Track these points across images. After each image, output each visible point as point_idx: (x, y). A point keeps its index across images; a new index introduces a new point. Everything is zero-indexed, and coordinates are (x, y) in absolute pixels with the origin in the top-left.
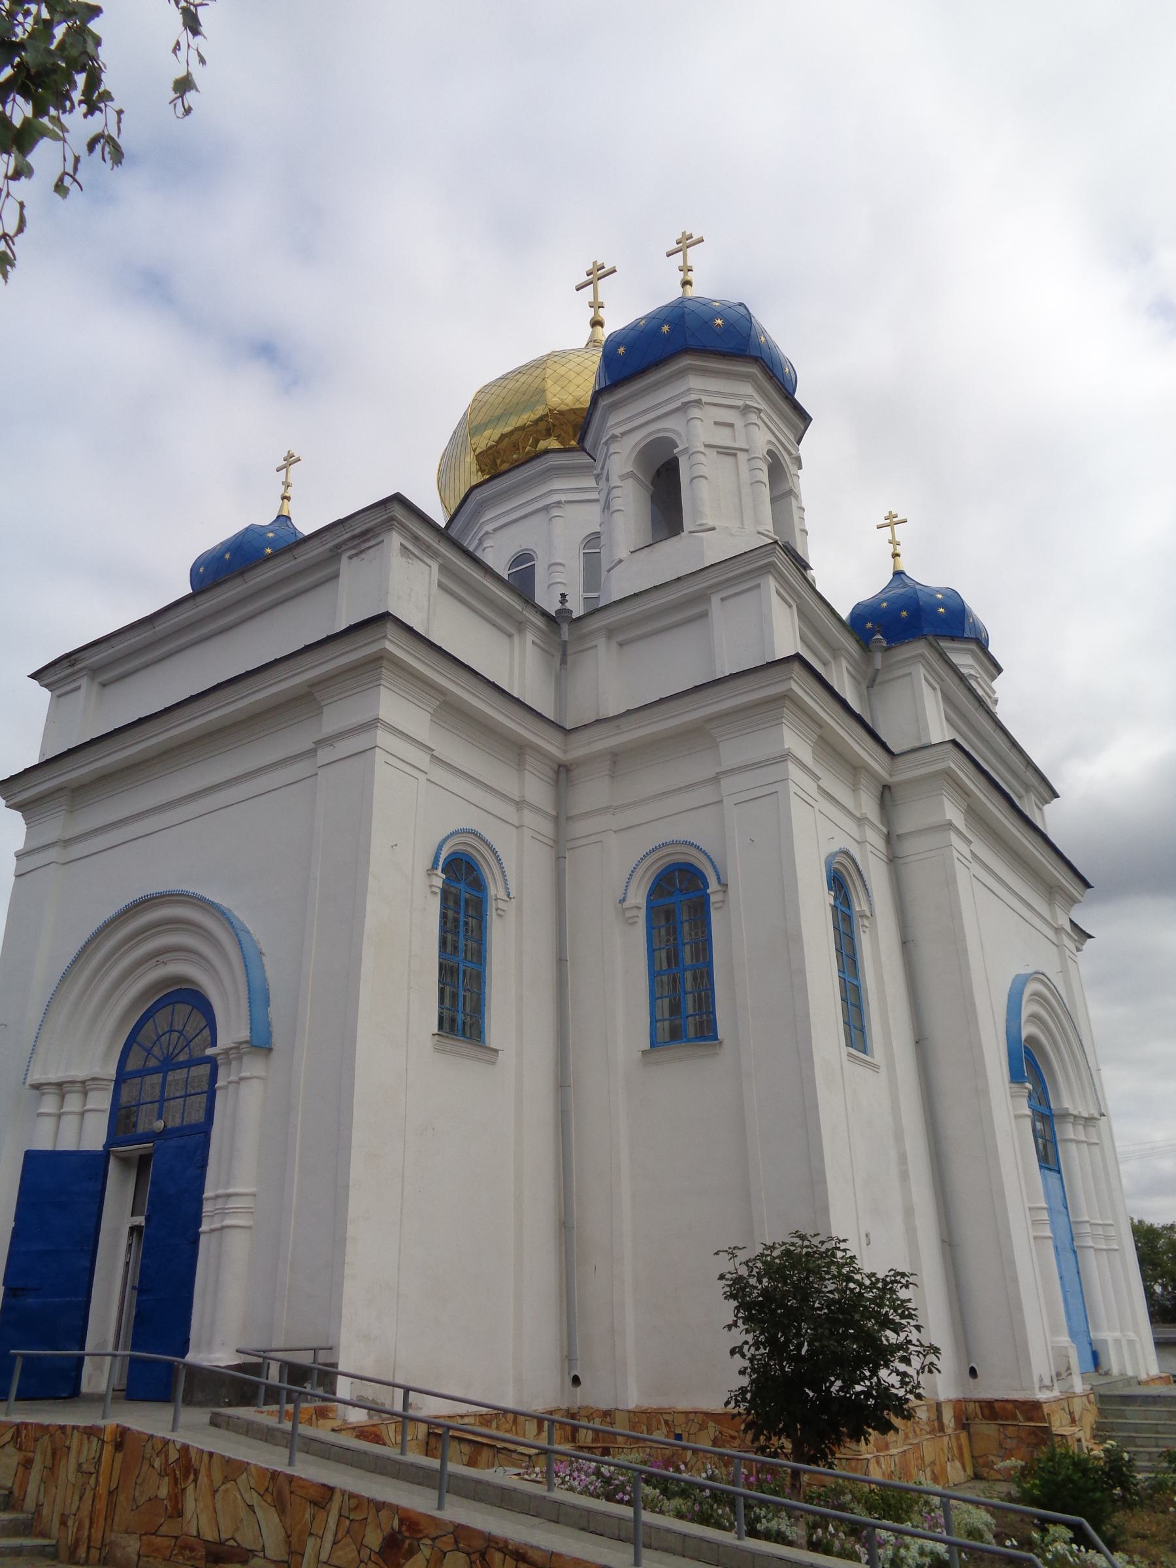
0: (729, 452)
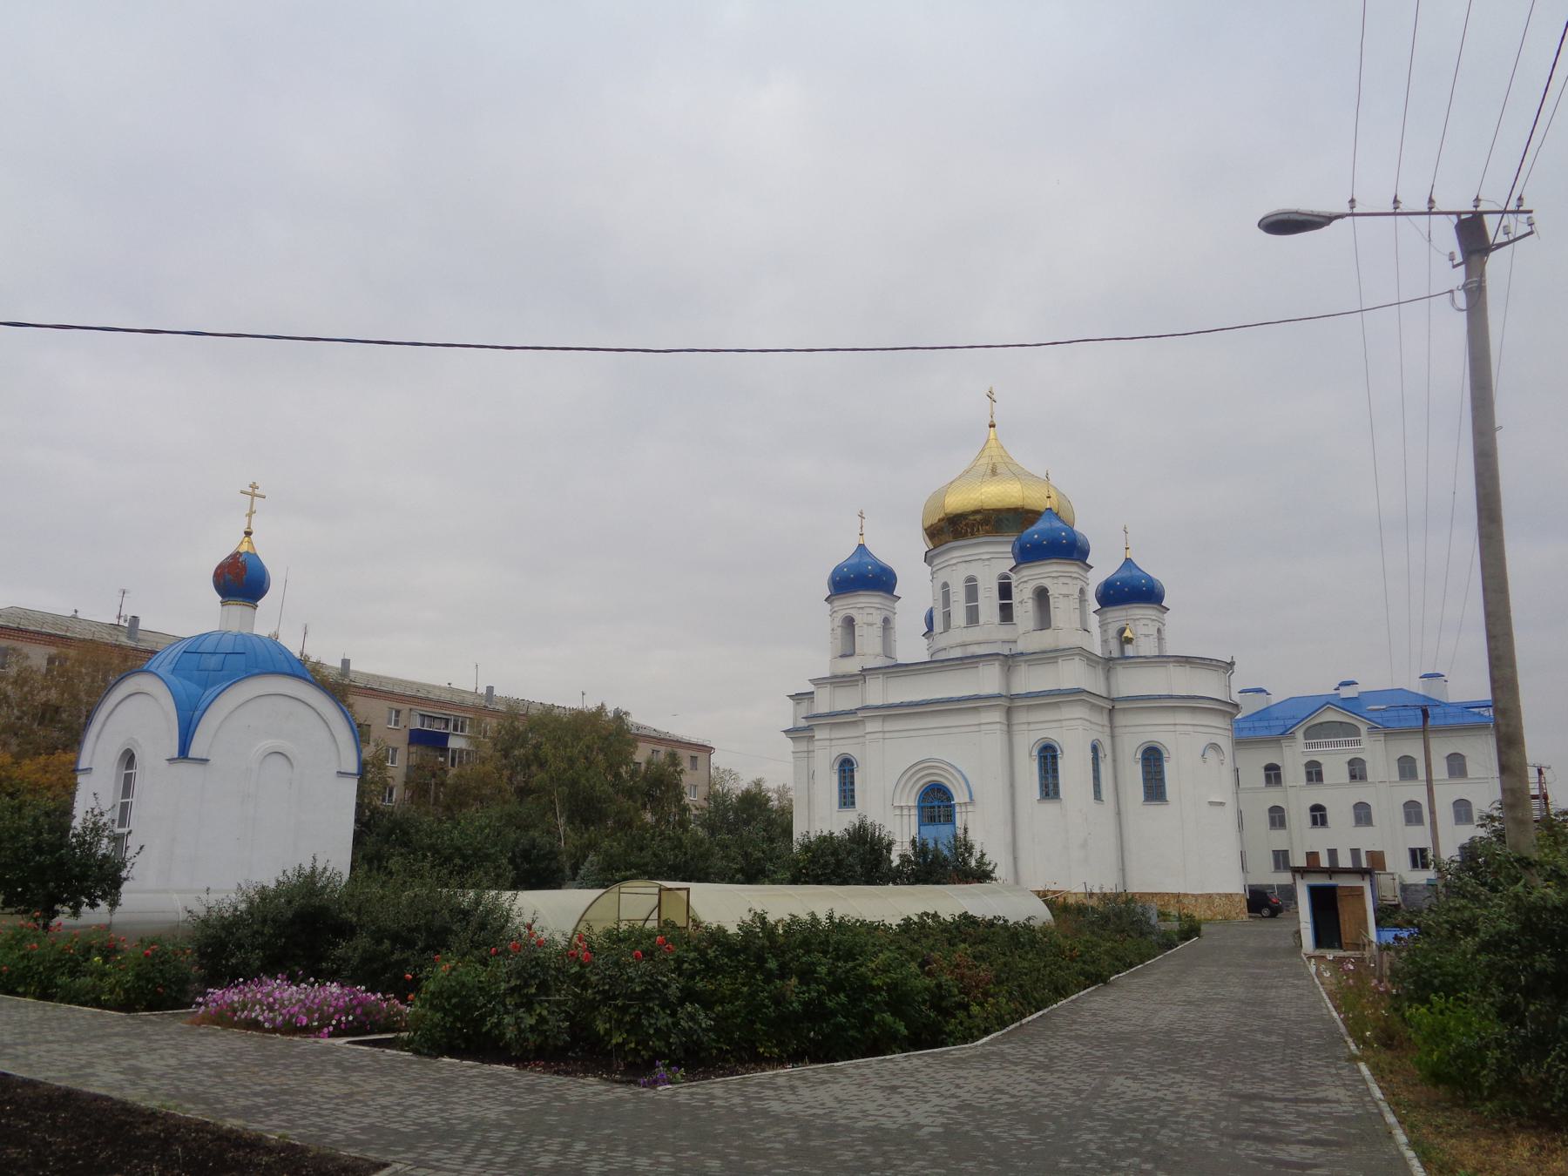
0: (1067, 596)
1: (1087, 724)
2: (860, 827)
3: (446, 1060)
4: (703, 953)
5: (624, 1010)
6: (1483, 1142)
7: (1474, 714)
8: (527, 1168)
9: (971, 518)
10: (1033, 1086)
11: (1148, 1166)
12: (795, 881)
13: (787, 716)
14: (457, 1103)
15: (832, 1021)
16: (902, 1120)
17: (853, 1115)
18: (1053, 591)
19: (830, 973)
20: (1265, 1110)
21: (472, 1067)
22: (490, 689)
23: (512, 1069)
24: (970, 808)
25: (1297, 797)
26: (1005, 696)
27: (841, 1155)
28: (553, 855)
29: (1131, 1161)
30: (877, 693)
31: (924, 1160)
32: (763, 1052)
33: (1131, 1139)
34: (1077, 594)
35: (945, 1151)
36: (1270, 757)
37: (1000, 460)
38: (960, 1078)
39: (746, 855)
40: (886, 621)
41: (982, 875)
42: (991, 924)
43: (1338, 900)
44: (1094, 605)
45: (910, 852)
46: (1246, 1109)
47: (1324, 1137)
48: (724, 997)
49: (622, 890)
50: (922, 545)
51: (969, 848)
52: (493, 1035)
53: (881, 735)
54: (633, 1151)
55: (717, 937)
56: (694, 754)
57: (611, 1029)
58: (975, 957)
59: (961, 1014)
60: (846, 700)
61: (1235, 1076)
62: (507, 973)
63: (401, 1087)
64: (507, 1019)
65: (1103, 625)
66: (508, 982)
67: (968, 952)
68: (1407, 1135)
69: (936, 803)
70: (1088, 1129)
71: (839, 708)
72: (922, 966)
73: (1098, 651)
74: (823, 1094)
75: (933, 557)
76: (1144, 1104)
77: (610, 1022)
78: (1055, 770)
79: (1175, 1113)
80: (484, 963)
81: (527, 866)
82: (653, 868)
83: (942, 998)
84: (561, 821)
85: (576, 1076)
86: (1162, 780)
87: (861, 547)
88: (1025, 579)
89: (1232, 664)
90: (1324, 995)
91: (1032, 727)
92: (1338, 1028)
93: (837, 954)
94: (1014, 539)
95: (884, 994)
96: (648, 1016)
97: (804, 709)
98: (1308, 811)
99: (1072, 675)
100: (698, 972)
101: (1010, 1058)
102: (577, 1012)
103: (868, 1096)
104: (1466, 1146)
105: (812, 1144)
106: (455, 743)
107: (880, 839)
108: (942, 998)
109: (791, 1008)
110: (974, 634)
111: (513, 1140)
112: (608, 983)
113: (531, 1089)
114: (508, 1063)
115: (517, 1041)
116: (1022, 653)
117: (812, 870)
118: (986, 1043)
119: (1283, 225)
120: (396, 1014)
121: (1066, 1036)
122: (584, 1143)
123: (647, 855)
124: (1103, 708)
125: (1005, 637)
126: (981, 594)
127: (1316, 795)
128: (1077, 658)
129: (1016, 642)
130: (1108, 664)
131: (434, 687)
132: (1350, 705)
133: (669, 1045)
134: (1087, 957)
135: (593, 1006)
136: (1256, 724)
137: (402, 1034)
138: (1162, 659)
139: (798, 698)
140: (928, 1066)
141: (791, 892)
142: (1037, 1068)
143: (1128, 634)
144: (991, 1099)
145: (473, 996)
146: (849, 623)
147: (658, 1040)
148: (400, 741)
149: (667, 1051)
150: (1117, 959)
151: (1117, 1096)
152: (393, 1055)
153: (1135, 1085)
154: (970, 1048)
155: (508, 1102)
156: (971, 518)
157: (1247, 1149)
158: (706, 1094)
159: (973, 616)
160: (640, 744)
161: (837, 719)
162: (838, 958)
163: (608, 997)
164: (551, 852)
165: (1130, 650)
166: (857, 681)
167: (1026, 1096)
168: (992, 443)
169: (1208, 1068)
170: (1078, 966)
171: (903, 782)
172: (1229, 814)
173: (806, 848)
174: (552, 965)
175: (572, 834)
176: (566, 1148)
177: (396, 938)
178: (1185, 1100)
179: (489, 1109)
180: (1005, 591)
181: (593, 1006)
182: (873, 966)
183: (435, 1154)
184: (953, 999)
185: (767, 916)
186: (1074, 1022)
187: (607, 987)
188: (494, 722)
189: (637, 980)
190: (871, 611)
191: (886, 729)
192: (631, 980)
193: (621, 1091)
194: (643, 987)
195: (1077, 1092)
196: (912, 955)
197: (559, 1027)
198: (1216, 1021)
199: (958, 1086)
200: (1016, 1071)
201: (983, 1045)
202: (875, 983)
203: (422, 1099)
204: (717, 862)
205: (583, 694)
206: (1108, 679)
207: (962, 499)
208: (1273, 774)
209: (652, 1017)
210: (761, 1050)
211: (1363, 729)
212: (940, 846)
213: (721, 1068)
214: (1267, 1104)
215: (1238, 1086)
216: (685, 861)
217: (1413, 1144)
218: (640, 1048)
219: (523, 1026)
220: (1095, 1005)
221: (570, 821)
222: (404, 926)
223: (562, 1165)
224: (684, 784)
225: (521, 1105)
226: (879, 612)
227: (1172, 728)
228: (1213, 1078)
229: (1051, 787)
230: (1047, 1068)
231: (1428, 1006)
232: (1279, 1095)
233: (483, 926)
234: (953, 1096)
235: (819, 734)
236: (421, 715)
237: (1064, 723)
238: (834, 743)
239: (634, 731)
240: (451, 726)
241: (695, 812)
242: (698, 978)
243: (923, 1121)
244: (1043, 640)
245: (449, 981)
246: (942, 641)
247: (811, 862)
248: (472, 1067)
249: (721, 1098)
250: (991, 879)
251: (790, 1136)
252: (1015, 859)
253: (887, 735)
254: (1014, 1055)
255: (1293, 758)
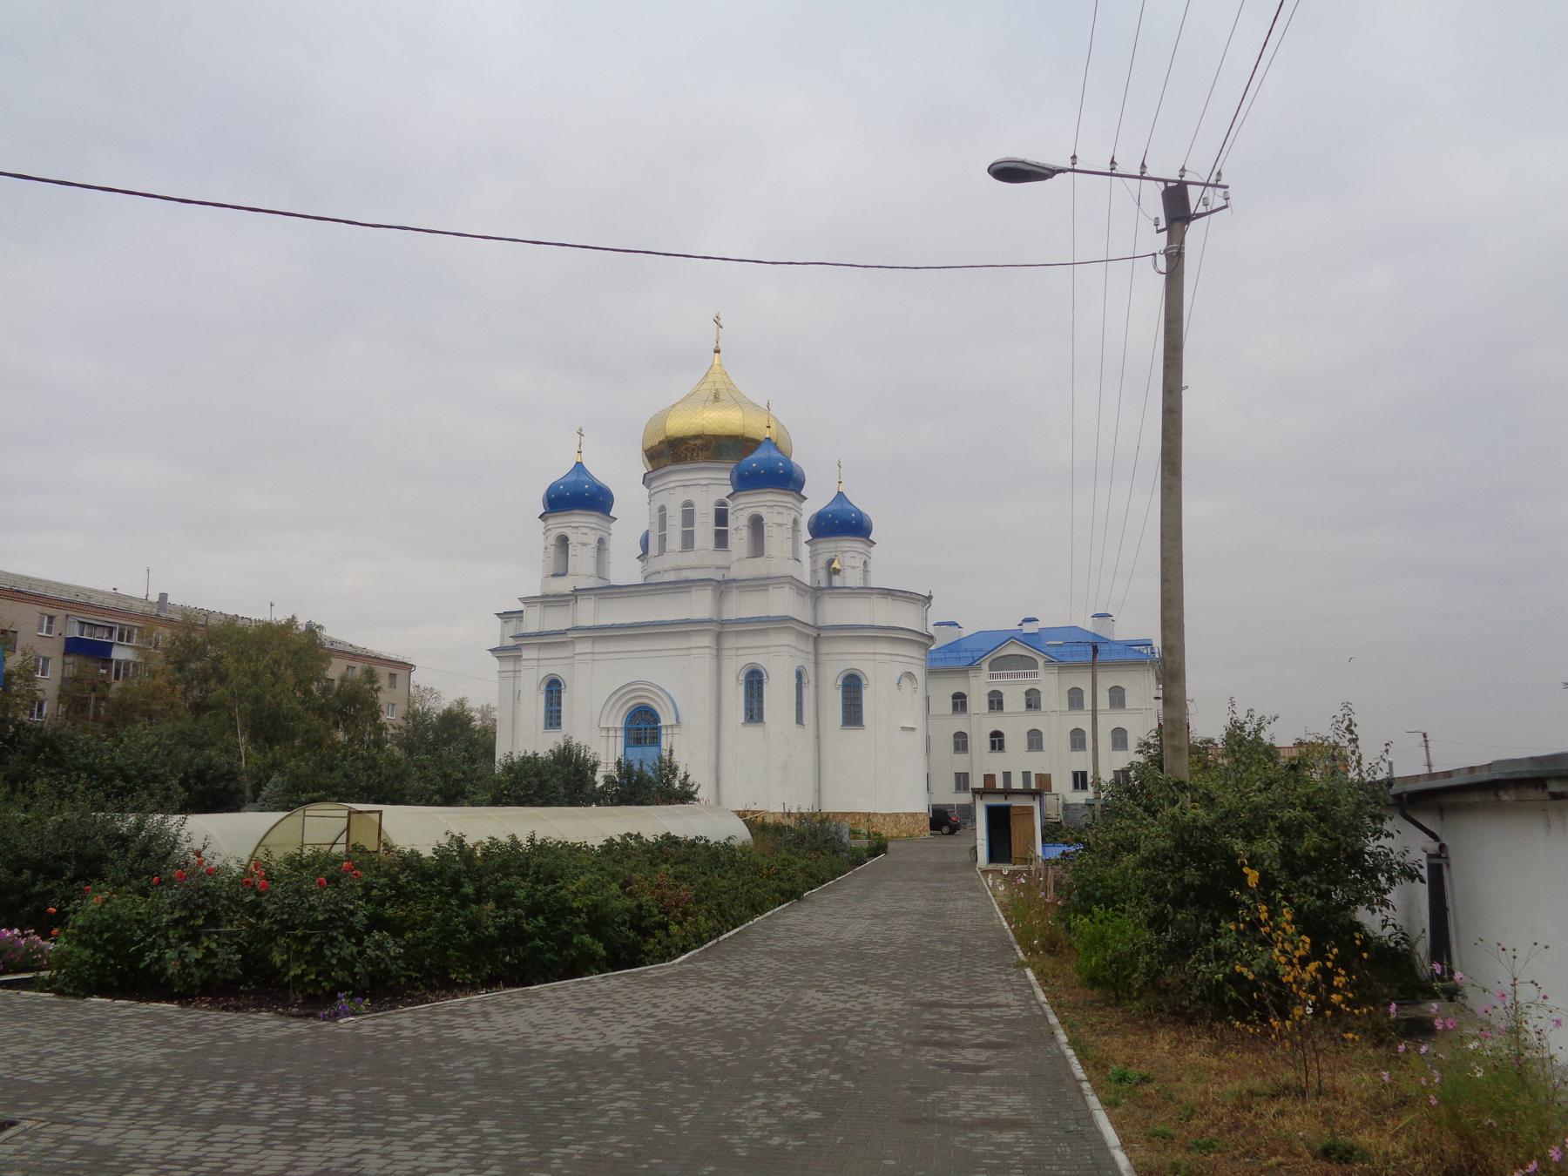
0: (778, 525)
1: (794, 651)
2: (565, 748)
3: (96, 1000)
4: (394, 879)
5: (305, 940)
6: (1131, 1038)
7: (1134, 650)
8: (185, 1117)
9: (692, 442)
10: (728, 1002)
11: (836, 1077)
12: (496, 802)
13: (495, 634)
14: (104, 1048)
15: (529, 945)
16: (598, 1043)
17: (546, 1040)
18: (769, 518)
19: (528, 896)
20: (944, 1016)
21: (124, 1007)
22: (163, 596)
23: (173, 1007)
24: (676, 731)
25: (980, 723)
26: (717, 622)
27: (535, 1082)
28: (231, 775)
29: (820, 1072)
30: (587, 614)
31: (619, 1082)
32: (456, 978)
33: (821, 1051)
34: (790, 525)
35: (640, 1073)
36: (957, 686)
37: (723, 387)
38: (657, 997)
39: (445, 776)
40: (601, 541)
41: (685, 796)
42: (693, 844)
43: (1012, 816)
44: (806, 536)
45: (615, 774)
46: (927, 1016)
47: (996, 1040)
48: (415, 923)
49: (307, 813)
50: (641, 467)
51: (673, 770)
52: (153, 971)
53: (590, 656)
54: (309, 1090)
55: (411, 862)
56: (393, 671)
57: (288, 960)
58: (676, 877)
59: (660, 934)
60: (556, 620)
61: (918, 985)
62: (170, 903)
63: (38, 1032)
64: (169, 954)
65: (813, 555)
66: (172, 913)
67: (670, 872)
68: (1067, 1035)
69: (643, 725)
70: (780, 1042)
71: (548, 627)
72: (623, 887)
73: (807, 580)
74: (518, 1020)
75: (652, 480)
76: (834, 1015)
77: (288, 953)
78: (761, 695)
79: (862, 1023)
80: (144, 893)
81: (200, 787)
82: (344, 789)
83: (642, 918)
84: (242, 740)
85: (247, 1011)
86: (860, 706)
87: (579, 465)
88: (742, 506)
89: (929, 598)
90: (996, 906)
91: (740, 652)
92: (1008, 936)
93: (537, 877)
94: (732, 466)
95: (583, 915)
96: (331, 945)
97: (512, 628)
98: (988, 736)
99: (782, 603)
100: (389, 898)
101: (707, 975)
102: (251, 944)
103: (563, 1020)
104: (1117, 1042)
105: (504, 1072)
106: (119, 654)
107: (585, 760)
108: (642, 918)
109: (486, 933)
110: (689, 559)
111: (170, 1086)
112: (287, 912)
113: (195, 1028)
114: (169, 1000)
115: (180, 976)
116: (735, 580)
117: (514, 791)
118: (683, 962)
119: (1009, 172)
120: (35, 953)
121: (761, 952)
122: (252, 1085)
123: (337, 776)
124: (808, 635)
125: (719, 563)
126: (698, 519)
127: (996, 722)
128: (787, 586)
129: (729, 568)
130: (816, 593)
131: (97, 592)
132: (1030, 640)
133: (353, 975)
134: (783, 875)
135: (269, 937)
136: (948, 655)
137: (42, 974)
138: (866, 591)
139: (505, 616)
140: (624, 987)
141: (491, 814)
142: (733, 984)
143: (836, 565)
144: (687, 1017)
145: (129, 930)
146: (563, 541)
147: (341, 970)
148: (53, 650)
149: (350, 981)
150: (811, 876)
151: (808, 1009)
152: (31, 997)
153: (825, 998)
154: (668, 967)
155: (167, 1043)
156: (692, 442)
157: (928, 1055)
158: (394, 1025)
159: (688, 541)
160: (333, 659)
161: (546, 639)
162: (538, 881)
163: (286, 927)
164: (230, 771)
165: (837, 581)
166: (568, 601)
167: (721, 1013)
168: (717, 369)
169: (892, 978)
170: (773, 884)
171: (609, 706)
172: (918, 740)
173: (509, 769)
174: (224, 894)
175: (255, 754)
176: (232, 1090)
177: (38, 868)
178: (871, 1010)
179: (142, 1053)
180: (721, 517)
181: (269, 937)
182: (574, 888)
183: (74, 1107)
184: (653, 919)
185: (465, 839)
186: (770, 938)
187: (285, 917)
188: (168, 632)
189: (319, 909)
190: (585, 530)
191: (595, 651)
192: (312, 908)
193: (298, 1026)
194: (326, 916)
195: (771, 1006)
196: (614, 877)
197: (230, 960)
198: (899, 933)
199: (655, 1005)
200: (712, 988)
201: (680, 963)
202: (575, 905)
203: (62, 1045)
204: (414, 784)
205: (272, 605)
206: (815, 607)
207: (685, 422)
208: (960, 702)
209: (335, 947)
210: (454, 976)
211: (1041, 662)
212: (645, 768)
213: (410, 996)
214: (945, 1011)
215: (919, 995)
216: (379, 782)
217: (1073, 1043)
218: (320, 979)
219: (187, 960)
220: (789, 921)
221: (253, 739)
222: (49, 854)
223: (226, 1111)
224: (380, 702)
225: (184, 1046)
226: (593, 532)
227: (872, 657)
228: (896, 987)
229: (756, 711)
230: (741, 984)
231: (1090, 916)
232: (955, 1002)
233: (145, 853)
234: (650, 1016)
235: (526, 654)
236: (81, 622)
237: (772, 649)
238: (542, 663)
239: (328, 646)
240: (116, 635)
241: (392, 731)
242: (387, 905)
243: (619, 1043)
244: (757, 568)
245: (100, 914)
246: (657, 564)
247: (513, 783)
248: (124, 1007)
249: (407, 1028)
250: (694, 799)
251: (479, 1065)
252: (718, 780)
253: (597, 657)
254: (710, 972)
255: (978, 688)
